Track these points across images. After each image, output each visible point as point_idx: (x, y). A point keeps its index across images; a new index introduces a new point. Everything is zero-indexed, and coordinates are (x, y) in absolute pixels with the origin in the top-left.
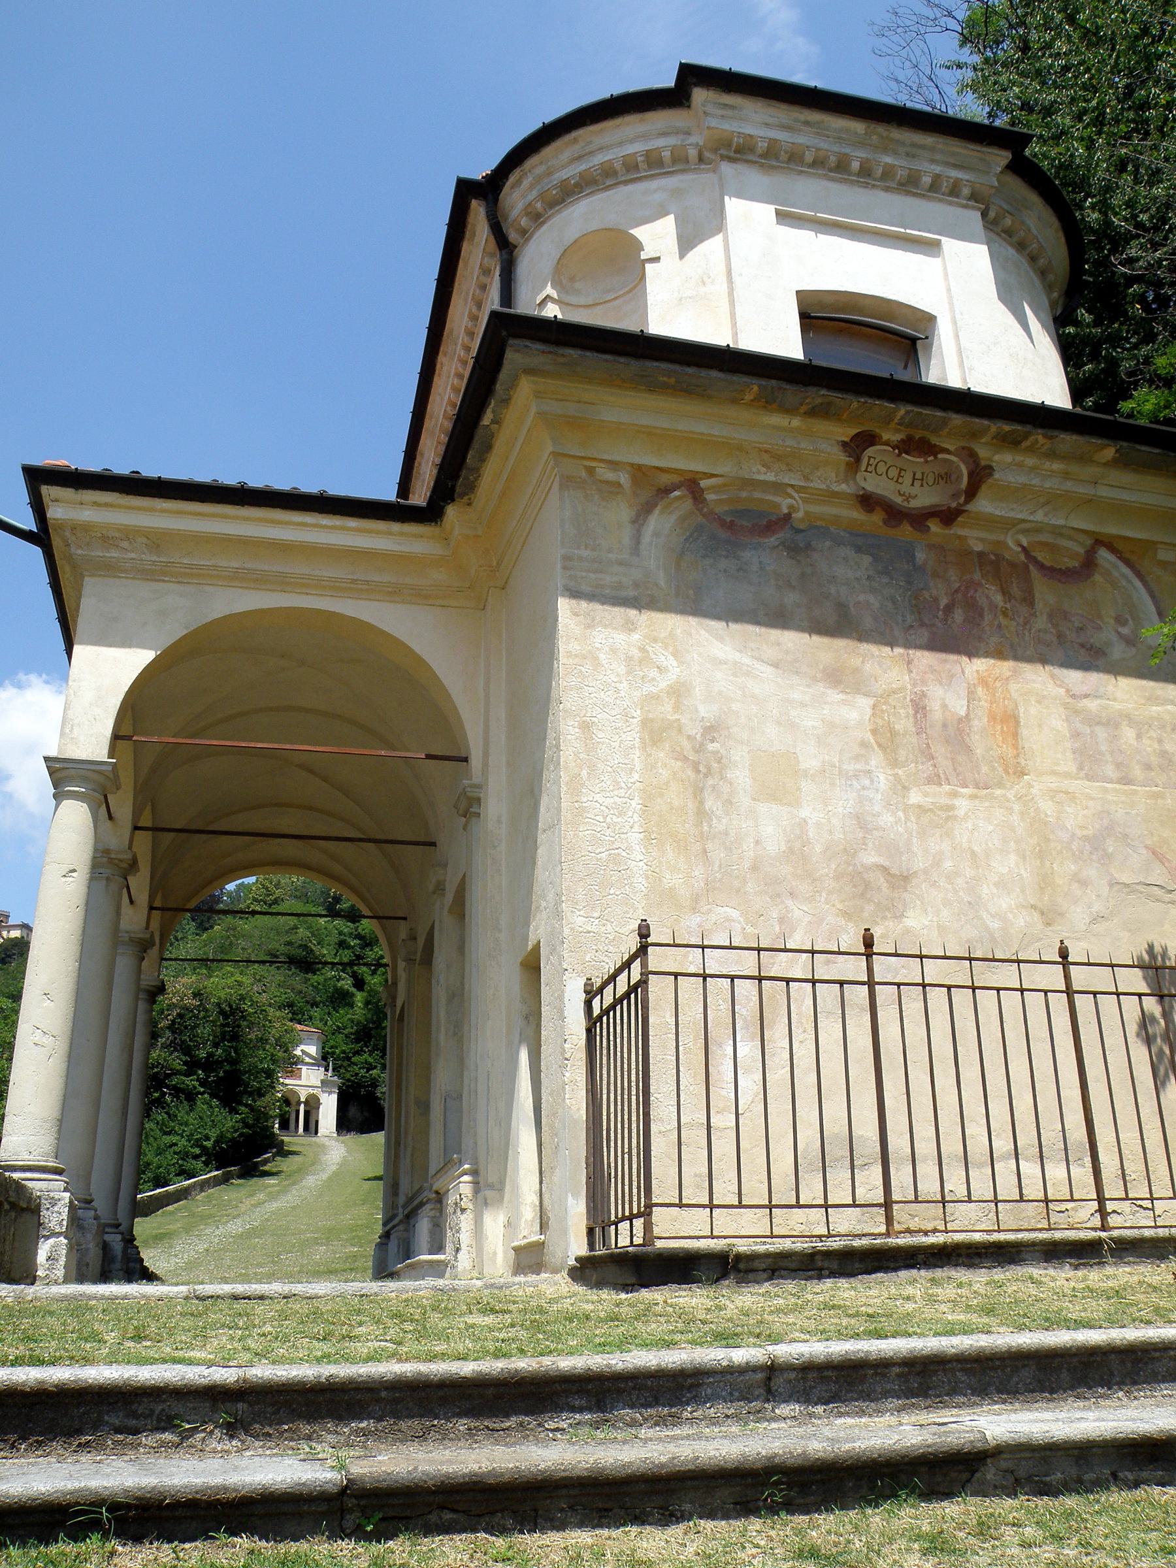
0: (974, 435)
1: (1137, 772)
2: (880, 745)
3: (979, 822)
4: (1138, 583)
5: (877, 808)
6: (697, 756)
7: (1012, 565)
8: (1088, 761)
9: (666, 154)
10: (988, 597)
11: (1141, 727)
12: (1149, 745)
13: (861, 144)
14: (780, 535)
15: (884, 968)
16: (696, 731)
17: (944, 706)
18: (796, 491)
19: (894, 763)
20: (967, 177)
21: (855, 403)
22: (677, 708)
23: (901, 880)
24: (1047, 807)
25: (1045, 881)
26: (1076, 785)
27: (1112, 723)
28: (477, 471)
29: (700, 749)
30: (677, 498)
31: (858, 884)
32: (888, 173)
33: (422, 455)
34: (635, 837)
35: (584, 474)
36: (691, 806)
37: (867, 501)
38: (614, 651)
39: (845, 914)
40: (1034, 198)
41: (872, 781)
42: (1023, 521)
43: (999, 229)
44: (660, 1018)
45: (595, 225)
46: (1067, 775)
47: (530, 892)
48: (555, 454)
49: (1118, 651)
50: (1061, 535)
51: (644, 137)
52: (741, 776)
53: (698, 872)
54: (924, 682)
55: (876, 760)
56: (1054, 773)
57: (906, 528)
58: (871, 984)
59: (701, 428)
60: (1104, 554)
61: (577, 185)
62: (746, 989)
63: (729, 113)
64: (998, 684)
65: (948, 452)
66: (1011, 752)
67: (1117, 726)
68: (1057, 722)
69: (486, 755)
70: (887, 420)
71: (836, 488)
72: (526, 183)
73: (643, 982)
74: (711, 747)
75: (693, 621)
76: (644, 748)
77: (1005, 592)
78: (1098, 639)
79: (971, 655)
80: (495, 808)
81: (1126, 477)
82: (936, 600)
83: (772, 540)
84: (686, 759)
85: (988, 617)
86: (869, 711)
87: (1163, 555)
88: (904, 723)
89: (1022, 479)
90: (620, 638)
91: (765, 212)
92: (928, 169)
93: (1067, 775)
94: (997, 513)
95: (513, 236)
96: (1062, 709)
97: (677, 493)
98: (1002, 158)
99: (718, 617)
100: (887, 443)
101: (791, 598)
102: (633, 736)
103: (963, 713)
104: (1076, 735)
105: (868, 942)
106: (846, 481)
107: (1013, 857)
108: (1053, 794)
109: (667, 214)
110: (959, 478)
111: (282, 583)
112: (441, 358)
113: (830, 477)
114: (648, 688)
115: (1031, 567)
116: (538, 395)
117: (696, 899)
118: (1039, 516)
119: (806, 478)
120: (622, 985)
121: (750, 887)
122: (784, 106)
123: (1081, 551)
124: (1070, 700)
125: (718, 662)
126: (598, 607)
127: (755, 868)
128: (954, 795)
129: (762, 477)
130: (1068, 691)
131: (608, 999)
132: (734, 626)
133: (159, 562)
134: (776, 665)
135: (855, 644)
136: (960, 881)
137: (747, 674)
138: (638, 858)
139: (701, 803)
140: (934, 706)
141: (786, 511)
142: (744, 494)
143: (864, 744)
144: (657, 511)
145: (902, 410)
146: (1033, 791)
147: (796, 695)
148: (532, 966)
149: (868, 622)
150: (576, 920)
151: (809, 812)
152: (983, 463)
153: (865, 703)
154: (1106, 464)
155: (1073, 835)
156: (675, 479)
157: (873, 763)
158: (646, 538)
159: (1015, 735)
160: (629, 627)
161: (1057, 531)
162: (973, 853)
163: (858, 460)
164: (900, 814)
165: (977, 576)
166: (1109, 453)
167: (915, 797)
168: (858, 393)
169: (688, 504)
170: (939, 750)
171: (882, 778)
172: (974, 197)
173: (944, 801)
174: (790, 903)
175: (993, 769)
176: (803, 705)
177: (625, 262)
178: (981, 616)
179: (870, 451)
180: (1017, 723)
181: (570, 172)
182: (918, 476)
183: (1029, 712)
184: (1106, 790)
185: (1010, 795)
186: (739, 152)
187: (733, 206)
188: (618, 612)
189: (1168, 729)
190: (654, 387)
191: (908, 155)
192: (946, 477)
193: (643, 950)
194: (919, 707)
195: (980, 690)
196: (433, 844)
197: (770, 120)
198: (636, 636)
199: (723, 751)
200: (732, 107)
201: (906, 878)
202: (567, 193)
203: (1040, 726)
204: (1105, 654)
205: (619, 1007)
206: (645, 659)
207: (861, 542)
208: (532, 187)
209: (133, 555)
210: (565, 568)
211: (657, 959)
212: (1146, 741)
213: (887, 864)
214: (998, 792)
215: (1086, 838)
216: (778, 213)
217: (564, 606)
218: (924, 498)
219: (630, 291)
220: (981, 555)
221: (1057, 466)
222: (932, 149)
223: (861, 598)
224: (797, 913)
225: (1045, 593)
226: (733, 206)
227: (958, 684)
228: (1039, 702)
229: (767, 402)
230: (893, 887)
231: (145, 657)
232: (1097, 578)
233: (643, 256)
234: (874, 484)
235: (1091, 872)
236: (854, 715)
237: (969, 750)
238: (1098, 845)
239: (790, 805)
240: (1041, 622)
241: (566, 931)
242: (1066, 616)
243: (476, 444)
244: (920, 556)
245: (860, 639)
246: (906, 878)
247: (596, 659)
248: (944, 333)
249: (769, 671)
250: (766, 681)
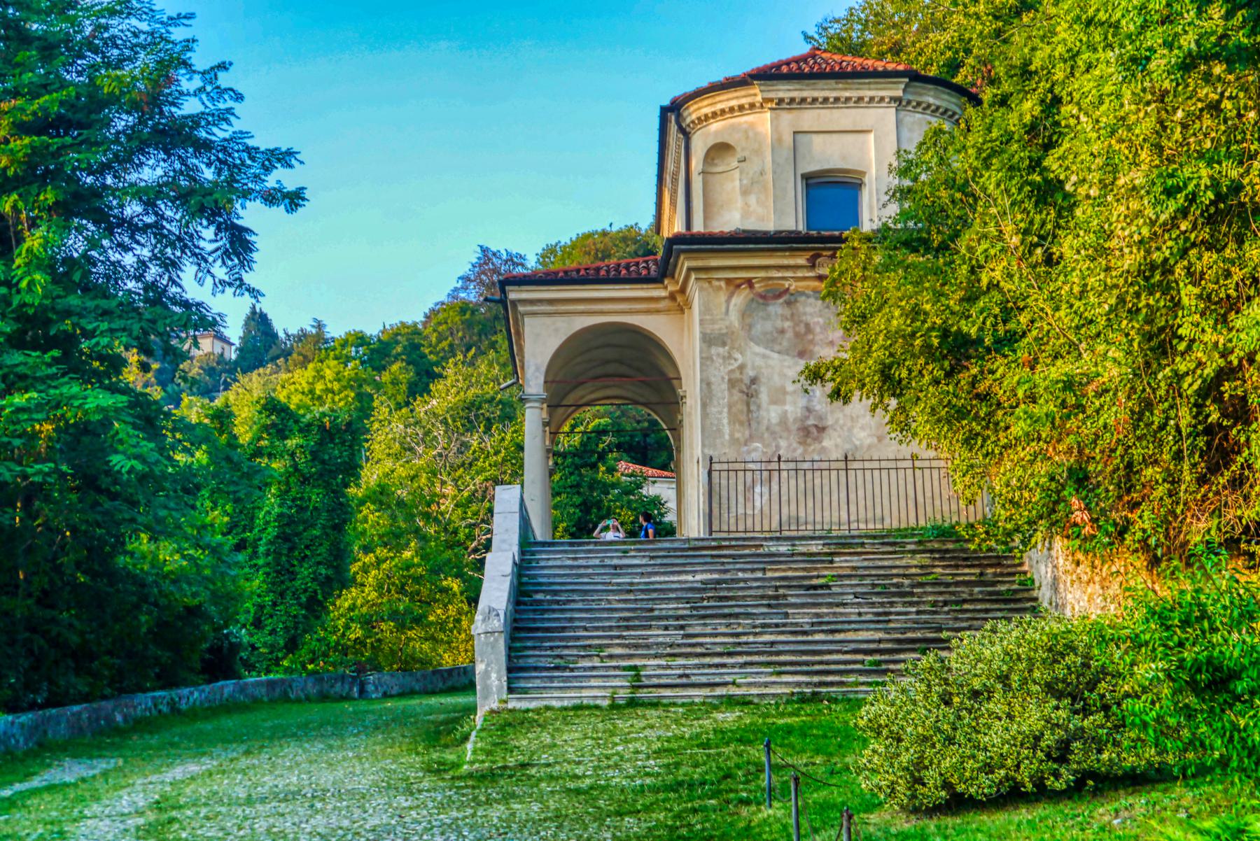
16: (748, 382)
23: (822, 430)
29: (749, 387)
32: (848, 99)
34: (725, 421)
36: (745, 409)
38: (718, 355)
39: (800, 443)
52: (764, 397)
53: (747, 433)
83: (781, 301)
90: (721, 350)
92: (867, 93)
102: (725, 386)
111: (602, 313)
114: (731, 368)
125: (757, 354)
127: (768, 429)
138: (726, 430)
151: (788, 408)
158: (731, 307)
162: (852, 418)
181: (708, 110)
206: (730, 357)
249: (776, 355)
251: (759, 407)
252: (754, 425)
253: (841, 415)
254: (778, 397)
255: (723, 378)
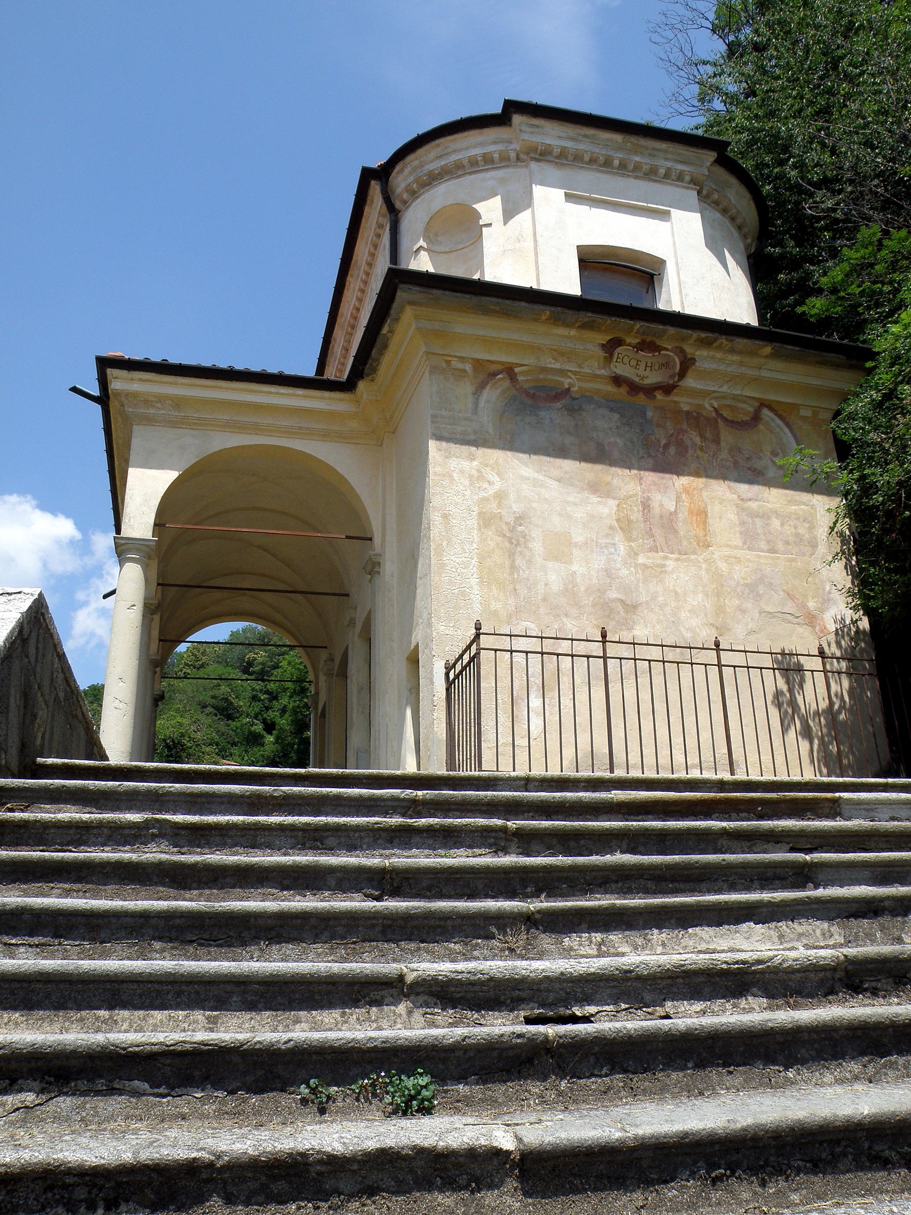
0: (684, 339)
1: (780, 546)
2: (621, 528)
3: (681, 575)
4: (787, 430)
5: (618, 566)
6: (510, 534)
7: (708, 419)
8: (749, 539)
9: (496, 156)
10: (691, 439)
11: (784, 518)
12: (788, 530)
13: (620, 149)
14: (564, 401)
15: (612, 650)
16: (510, 519)
17: (661, 505)
18: (575, 375)
19: (630, 539)
20: (688, 169)
21: (609, 321)
22: (499, 506)
23: (632, 608)
24: (723, 566)
25: (720, 610)
26: (741, 553)
27: (765, 516)
28: (378, 361)
29: (513, 530)
30: (500, 379)
31: (606, 608)
32: (637, 167)
33: (335, 340)
34: (474, 581)
35: (444, 365)
36: (507, 563)
37: (617, 380)
38: (462, 472)
40: (733, 181)
41: (616, 550)
42: (715, 392)
43: (708, 200)
44: (487, 685)
45: (451, 201)
46: (736, 547)
47: (412, 616)
48: (427, 353)
49: (771, 473)
50: (739, 401)
51: (482, 144)
52: (537, 546)
54: (649, 491)
55: (619, 537)
56: (728, 546)
57: (642, 396)
58: (605, 658)
59: (516, 336)
60: (766, 412)
61: (439, 174)
62: (535, 659)
63: (536, 130)
64: (695, 492)
65: (667, 349)
66: (701, 533)
67: (769, 518)
68: (731, 515)
69: (384, 536)
70: (629, 331)
71: (598, 372)
72: (406, 171)
73: (478, 654)
74: (520, 529)
75: (509, 454)
76: (479, 529)
77: (701, 436)
78: (759, 465)
79: (679, 474)
80: (390, 568)
81: (779, 365)
82: (659, 441)
83: (558, 405)
84: (504, 536)
85: (690, 451)
86: (615, 508)
87: (805, 412)
88: (636, 515)
89: (714, 366)
90: (466, 464)
91: (558, 194)
92: (663, 165)
93: (736, 547)
94: (699, 387)
95: (398, 205)
96: (734, 508)
97: (500, 376)
98: (711, 156)
99: (524, 452)
100: (629, 345)
101: (569, 440)
102: (473, 522)
103: (673, 510)
104: (743, 523)
105: (604, 635)
106: (604, 368)
107: (700, 595)
108: (727, 559)
109: (496, 195)
110: (675, 365)
111: (256, 429)
112: (349, 278)
113: (594, 366)
114: (482, 494)
115: (719, 420)
116: (416, 317)
117: (510, 616)
118: (725, 389)
119: (580, 366)
120: (466, 658)
121: (542, 611)
122: (570, 125)
123: (752, 410)
124: (740, 502)
126: (452, 445)
127: (544, 600)
128: (666, 558)
129: (553, 366)
130: (739, 496)
131: (458, 667)
132: (533, 457)
133: (180, 416)
134: (559, 481)
135: (608, 467)
136: (668, 609)
137: (542, 486)
138: (476, 592)
139: (514, 561)
140: (655, 505)
141: (567, 387)
142: (542, 377)
143: (611, 528)
144: (488, 388)
145: (638, 325)
146: (714, 556)
147: (571, 499)
148: (414, 660)
149: (616, 454)
150: (440, 628)
152: (689, 356)
153: (613, 503)
154: (767, 357)
155: (738, 583)
156: (500, 367)
157: (617, 539)
158: (482, 403)
159: (705, 523)
160: (471, 458)
161: (735, 398)
162: (676, 593)
163: (611, 355)
164: (632, 569)
165: (685, 427)
166: (768, 350)
167: (641, 559)
168: (611, 315)
169: (507, 383)
170: (657, 532)
171: (622, 548)
172: (693, 181)
173: (660, 562)
174: (565, 620)
175: (690, 543)
176: (575, 504)
177: (468, 227)
178: (687, 450)
179: (619, 350)
180: (706, 516)
182: (649, 364)
183: (714, 510)
184: (760, 557)
185: (701, 558)
186: (542, 155)
187: (539, 191)
188: (465, 448)
189: (801, 520)
190: (486, 312)
191: (650, 155)
192: (666, 365)
193: (477, 636)
194: (646, 506)
195: (684, 496)
196: (348, 595)
197: (563, 135)
198: (475, 463)
199: (527, 532)
200: (538, 127)
201: (635, 607)
202: (433, 179)
203: (720, 517)
204: (763, 474)
205: (465, 670)
206: (481, 477)
207: (612, 405)
208: (410, 173)
209: (163, 412)
210: (432, 422)
211: (484, 641)
212: (786, 527)
213: (623, 598)
214: (693, 557)
215: (746, 585)
216: (566, 194)
217: (433, 445)
218: (653, 378)
219: (473, 244)
220: (688, 413)
221: (735, 358)
222: (666, 151)
223: (612, 440)
224: (569, 626)
225: (727, 436)
226: (539, 191)
227: (670, 492)
228: (721, 504)
229: (555, 320)
230: (627, 612)
231: (172, 475)
232: (761, 427)
233: (481, 223)
234: (622, 369)
235: (749, 605)
236: (606, 511)
237: (676, 531)
238: (753, 588)
239: (565, 563)
240: (724, 454)
241: (434, 634)
242: (740, 450)
243: (378, 345)
244: (649, 414)
245: (611, 465)
246: (635, 607)
247: (451, 476)
248: (670, 271)
249: (554, 484)
250: (553, 490)
251: (530, 562)
252: (523, 591)
253: (659, 588)
254: (560, 548)
255: (470, 510)
